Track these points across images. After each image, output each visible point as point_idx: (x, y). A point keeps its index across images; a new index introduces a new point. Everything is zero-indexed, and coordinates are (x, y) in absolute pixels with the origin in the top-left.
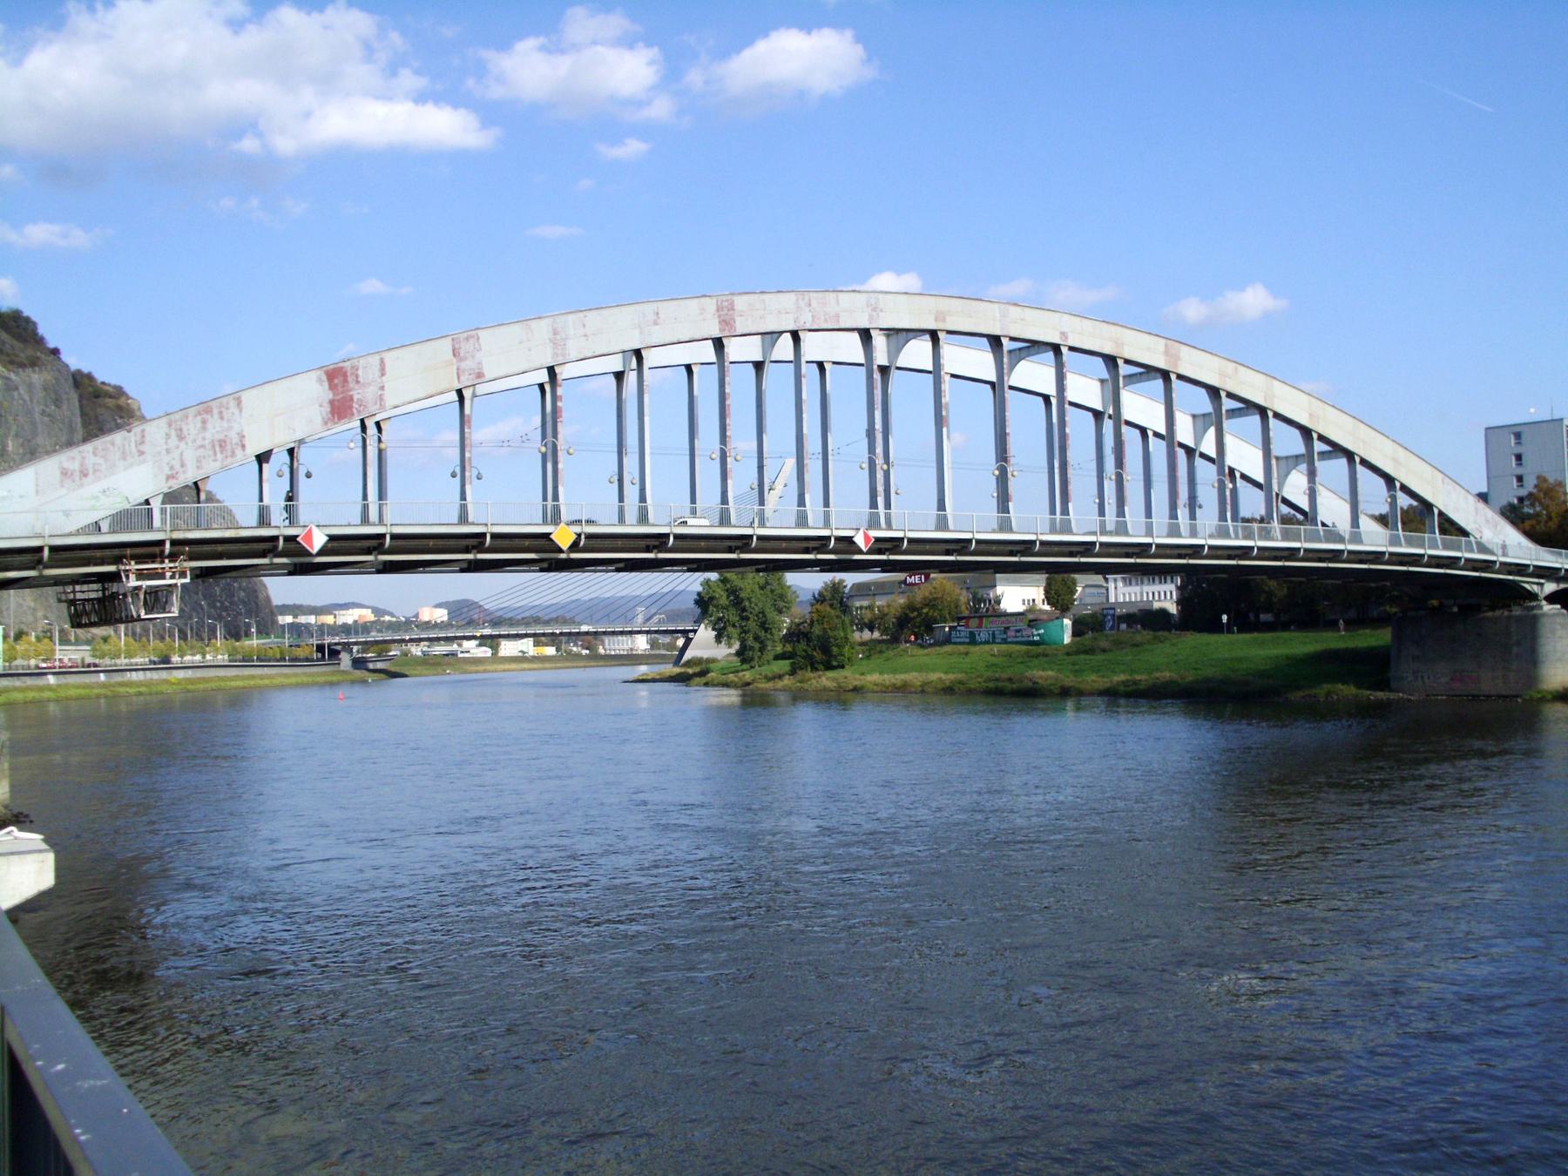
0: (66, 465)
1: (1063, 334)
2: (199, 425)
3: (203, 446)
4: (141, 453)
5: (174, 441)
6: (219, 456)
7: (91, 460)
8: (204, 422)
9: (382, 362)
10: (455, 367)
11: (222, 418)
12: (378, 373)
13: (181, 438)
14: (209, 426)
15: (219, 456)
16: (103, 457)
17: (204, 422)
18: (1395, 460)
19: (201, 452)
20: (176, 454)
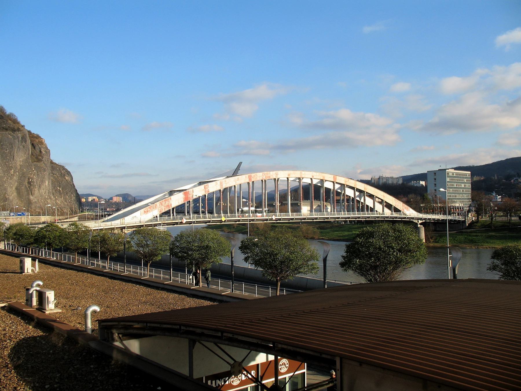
0: (145, 210)
1: (313, 176)
2: (165, 203)
3: (165, 206)
4: (156, 208)
5: (161, 206)
6: (168, 208)
7: (149, 209)
8: (165, 202)
9: (193, 190)
10: (204, 191)
11: (168, 201)
12: (192, 192)
13: (162, 205)
14: (166, 203)
15: (168, 208)
16: (151, 209)
17: (165, 202)
18: (384, 196)
19: (165, 207)
20: (161, 208)
